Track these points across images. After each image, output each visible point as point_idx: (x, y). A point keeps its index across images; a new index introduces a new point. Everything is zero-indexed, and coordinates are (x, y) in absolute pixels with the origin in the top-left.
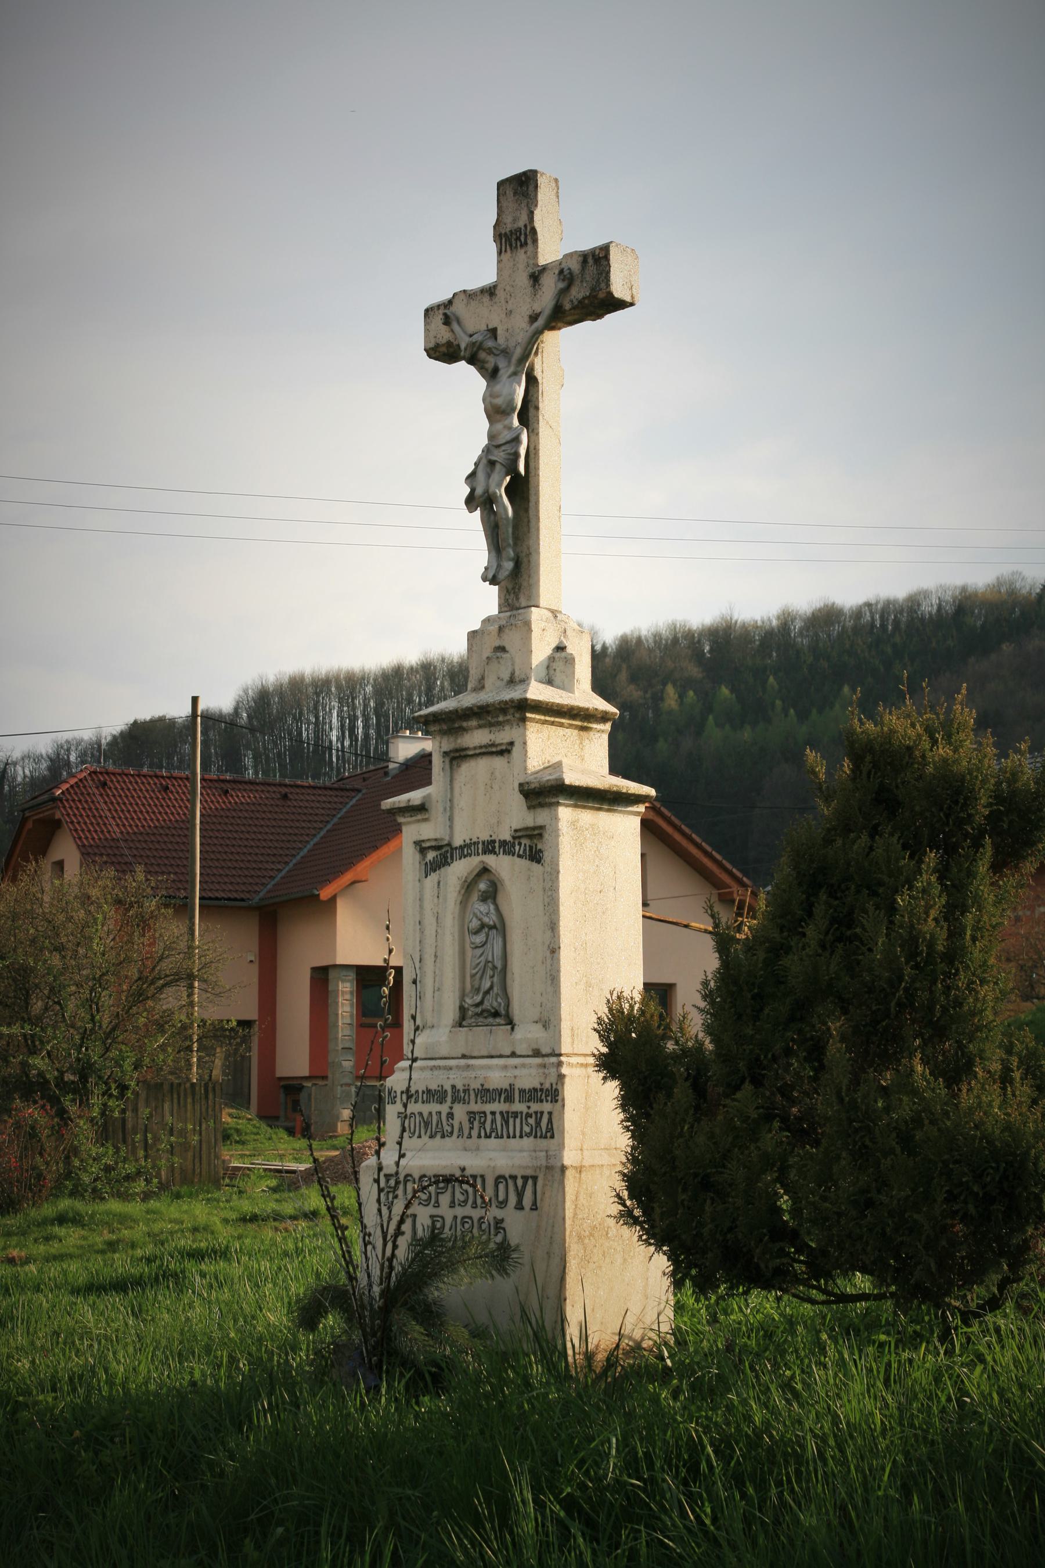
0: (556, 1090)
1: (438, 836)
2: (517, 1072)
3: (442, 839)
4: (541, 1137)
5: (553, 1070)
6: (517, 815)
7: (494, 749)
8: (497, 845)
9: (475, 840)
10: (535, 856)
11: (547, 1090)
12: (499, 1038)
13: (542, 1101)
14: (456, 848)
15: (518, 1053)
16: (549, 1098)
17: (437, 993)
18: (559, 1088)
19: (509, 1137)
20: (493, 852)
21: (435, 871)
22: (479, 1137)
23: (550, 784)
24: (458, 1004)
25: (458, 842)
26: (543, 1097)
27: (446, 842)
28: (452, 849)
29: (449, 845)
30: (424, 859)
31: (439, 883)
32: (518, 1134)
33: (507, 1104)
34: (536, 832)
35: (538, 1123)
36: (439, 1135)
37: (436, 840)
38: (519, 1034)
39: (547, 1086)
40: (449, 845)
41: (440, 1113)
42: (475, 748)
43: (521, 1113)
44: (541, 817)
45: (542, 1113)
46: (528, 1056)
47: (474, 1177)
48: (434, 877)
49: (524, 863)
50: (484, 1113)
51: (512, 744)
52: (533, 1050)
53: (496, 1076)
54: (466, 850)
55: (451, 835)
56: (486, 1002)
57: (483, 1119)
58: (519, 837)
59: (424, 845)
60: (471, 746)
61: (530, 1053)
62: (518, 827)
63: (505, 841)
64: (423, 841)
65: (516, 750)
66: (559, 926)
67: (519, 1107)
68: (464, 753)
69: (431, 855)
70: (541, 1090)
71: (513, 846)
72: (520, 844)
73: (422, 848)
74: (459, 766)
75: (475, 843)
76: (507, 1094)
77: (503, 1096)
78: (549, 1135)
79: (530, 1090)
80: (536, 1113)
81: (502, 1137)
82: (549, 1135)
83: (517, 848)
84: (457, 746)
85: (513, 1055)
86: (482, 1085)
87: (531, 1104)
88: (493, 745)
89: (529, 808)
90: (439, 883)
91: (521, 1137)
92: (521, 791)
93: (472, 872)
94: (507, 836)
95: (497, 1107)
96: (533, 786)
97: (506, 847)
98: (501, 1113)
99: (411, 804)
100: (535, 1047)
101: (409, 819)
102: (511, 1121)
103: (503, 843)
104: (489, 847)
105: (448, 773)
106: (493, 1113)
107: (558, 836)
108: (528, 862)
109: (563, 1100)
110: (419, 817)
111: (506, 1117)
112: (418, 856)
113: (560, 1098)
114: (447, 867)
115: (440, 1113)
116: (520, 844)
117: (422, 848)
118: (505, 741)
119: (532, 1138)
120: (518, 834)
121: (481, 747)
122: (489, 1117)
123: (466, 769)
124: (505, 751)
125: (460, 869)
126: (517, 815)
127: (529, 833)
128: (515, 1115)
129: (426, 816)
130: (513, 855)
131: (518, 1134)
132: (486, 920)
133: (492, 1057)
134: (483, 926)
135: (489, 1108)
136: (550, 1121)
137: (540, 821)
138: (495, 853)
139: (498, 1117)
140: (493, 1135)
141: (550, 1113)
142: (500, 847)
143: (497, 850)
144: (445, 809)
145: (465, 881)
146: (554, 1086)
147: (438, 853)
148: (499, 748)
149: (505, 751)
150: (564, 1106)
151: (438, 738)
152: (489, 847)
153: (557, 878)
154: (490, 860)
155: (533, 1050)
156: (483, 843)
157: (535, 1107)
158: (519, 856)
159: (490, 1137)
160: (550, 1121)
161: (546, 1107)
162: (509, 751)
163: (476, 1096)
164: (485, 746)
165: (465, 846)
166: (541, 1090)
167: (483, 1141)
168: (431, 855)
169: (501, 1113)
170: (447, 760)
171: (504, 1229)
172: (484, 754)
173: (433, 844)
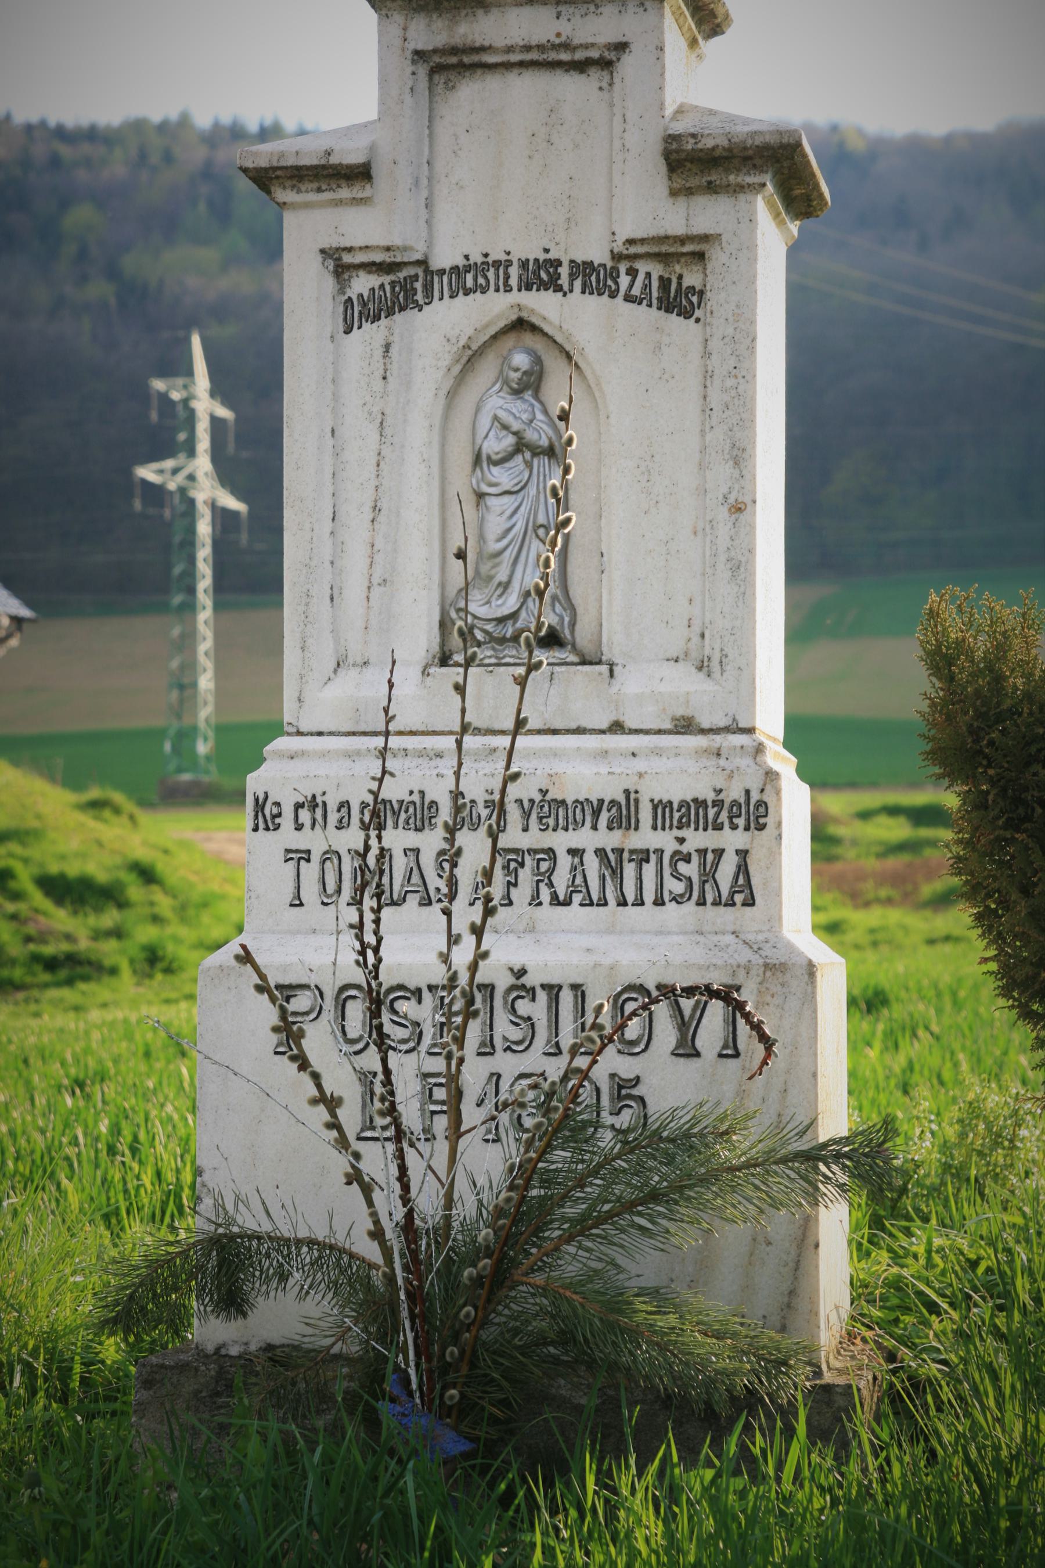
0: (762, 804)
1: (397, 242)
2: (640, 765)
3: (405, 249)
4: (716, 903)
5: (745, 762)
6: (645, 207)
7: (565, 57)
8: (564, 271)
9: (497, 255)
10: (679, 301)
11: (735, 803)
12: (562, 692)
13: (718, 827)
14: (442, 272)
15: (630, 723)
16: (741, 822)
17: (376, 591)
18: (769, 797)
19: (623, 903)
20: (553, 284)
21: (377, 318)
22: (535, 901)
23: (758, 141)
24: (437, 617)
25: (444, 258)
26: (724, 817)
27: (418, 256)
28: (428, 271)
29: (423, 263)
30: (342, 291)
31: (387, 347)
32: (649, 896)
33: (618, 834)
34: (688, 248)
35: (708, 875)
36: (413, 900)
37: (388, 249)
38: (632, 683)
39: (734, 793)
40: (423, 263)
41: (417, 851)
42: (510, 49)
43: (660, 852)
44: (706, 215)
45: (719, 853)
46: (659, 732)
47: (553, 990)
48: (372, 334)
49: (648, 316)
50: (551, 852)
51: (622, 47)
52: (674, 719)
53: (581, 771)
54: (470, 277)
55: (430, 242)
56: (523, 614)
57: (544, 866)
58: (636, 257)
59: (347, 259)
60: (500, 43)
61: (668, 725)
62: (639, 235)
63: (589, 265)
64: (349, 250)
65: (628, 65)
66: (752, 456)
67: (646, 838)
68: (475, 58)
69: (362, 284)
70: (718, 804)
71: (614, 274)
72: (632, 273)
73: (340, 264)
74: (450, 87)
75: (497, 264)
76: (623, 813)
77: (604, 817)
78: (739, 898)
79: (684, 804)
80: (703, 852)
81: (603, 903)
82: (739, 898)
83: (624, 280)
84: (457, 41)
85: (617, 727)
86: (544, 792)
87: (687, 833)
88: (566, 46)
89: (674, 193)
90: (387, 347)
91: (659, 902)
92: (667, 155)
93: (487, 326)
94: (599, 255)
95: (585, 838)
96: (709, 143)
97: (593, 278)
98: (600, 853)
99: (334, 160)
100: (680, 712)
101: (312, 197)
102: (629, 870)
103: (584, 270)
104: (542, 275)
105: (425, 101)
106: (575, 853)
107: (753, 260)
108: (655, 314)
109: (779, 824)
110: (344, 193)
111: (612, 863)
112: (330, 283)
113: (770, 820)
114: (411, 314)
115: (417, 851)
116: (632, 273)
117: (340, 264)
118: (602, 40)
119: (690, 907)
120: (633, 250)
121: (528, 48)
122: (564, 862)
123: (471, 94)
124: (603, 62)
125: (449, 321)
126: (645, 207)
127: (664, 249)
128: (642, 857)
129: (367, 192)
130: (613, 295)
131: (649, 896)
132: (530, 435)
133: (555, 732)
134: (521, 446)
135: (561, 841)
136: (743, 868)
137: (701, 225)
138: (559, 289)
139: (592, 865)
140: (577, 898)
141: (743, 854)
142: (572, 277)
143: (564, 280)
144: (417, 182)
145: (466, 347)
146: (755, 797)
147: (387, 279)
148: (579, 55)
149: (603, 62)
150: (780, 836)
151: (398, 18)
152: (542, 275)
153: (752, 349)
154: (543, 305)
155: (674, 719)
156: (524, 264)
157: (696, 839)
158: (629, 298)
159: (567, 903)
160: (743, 868)
161: (732, 840)
162: (606, 64)
163: (527, 815)
164: (541, 48)
165: (468, 269)
166: (718, 804)
167: (547, 911)
168: (362, 284)
169: (600, 853)
170: (422, 71)
171: (641, 1100)
172: (522, 64)
173: (378, 257)
